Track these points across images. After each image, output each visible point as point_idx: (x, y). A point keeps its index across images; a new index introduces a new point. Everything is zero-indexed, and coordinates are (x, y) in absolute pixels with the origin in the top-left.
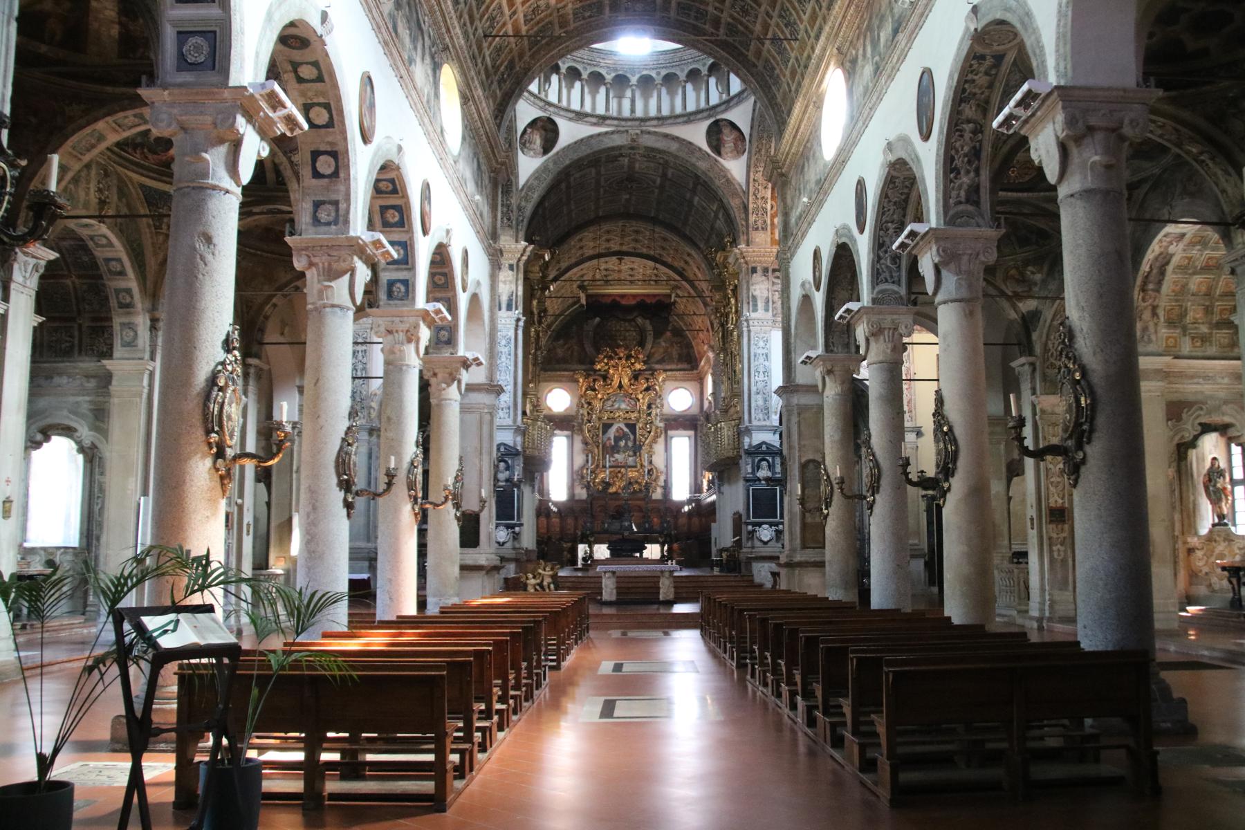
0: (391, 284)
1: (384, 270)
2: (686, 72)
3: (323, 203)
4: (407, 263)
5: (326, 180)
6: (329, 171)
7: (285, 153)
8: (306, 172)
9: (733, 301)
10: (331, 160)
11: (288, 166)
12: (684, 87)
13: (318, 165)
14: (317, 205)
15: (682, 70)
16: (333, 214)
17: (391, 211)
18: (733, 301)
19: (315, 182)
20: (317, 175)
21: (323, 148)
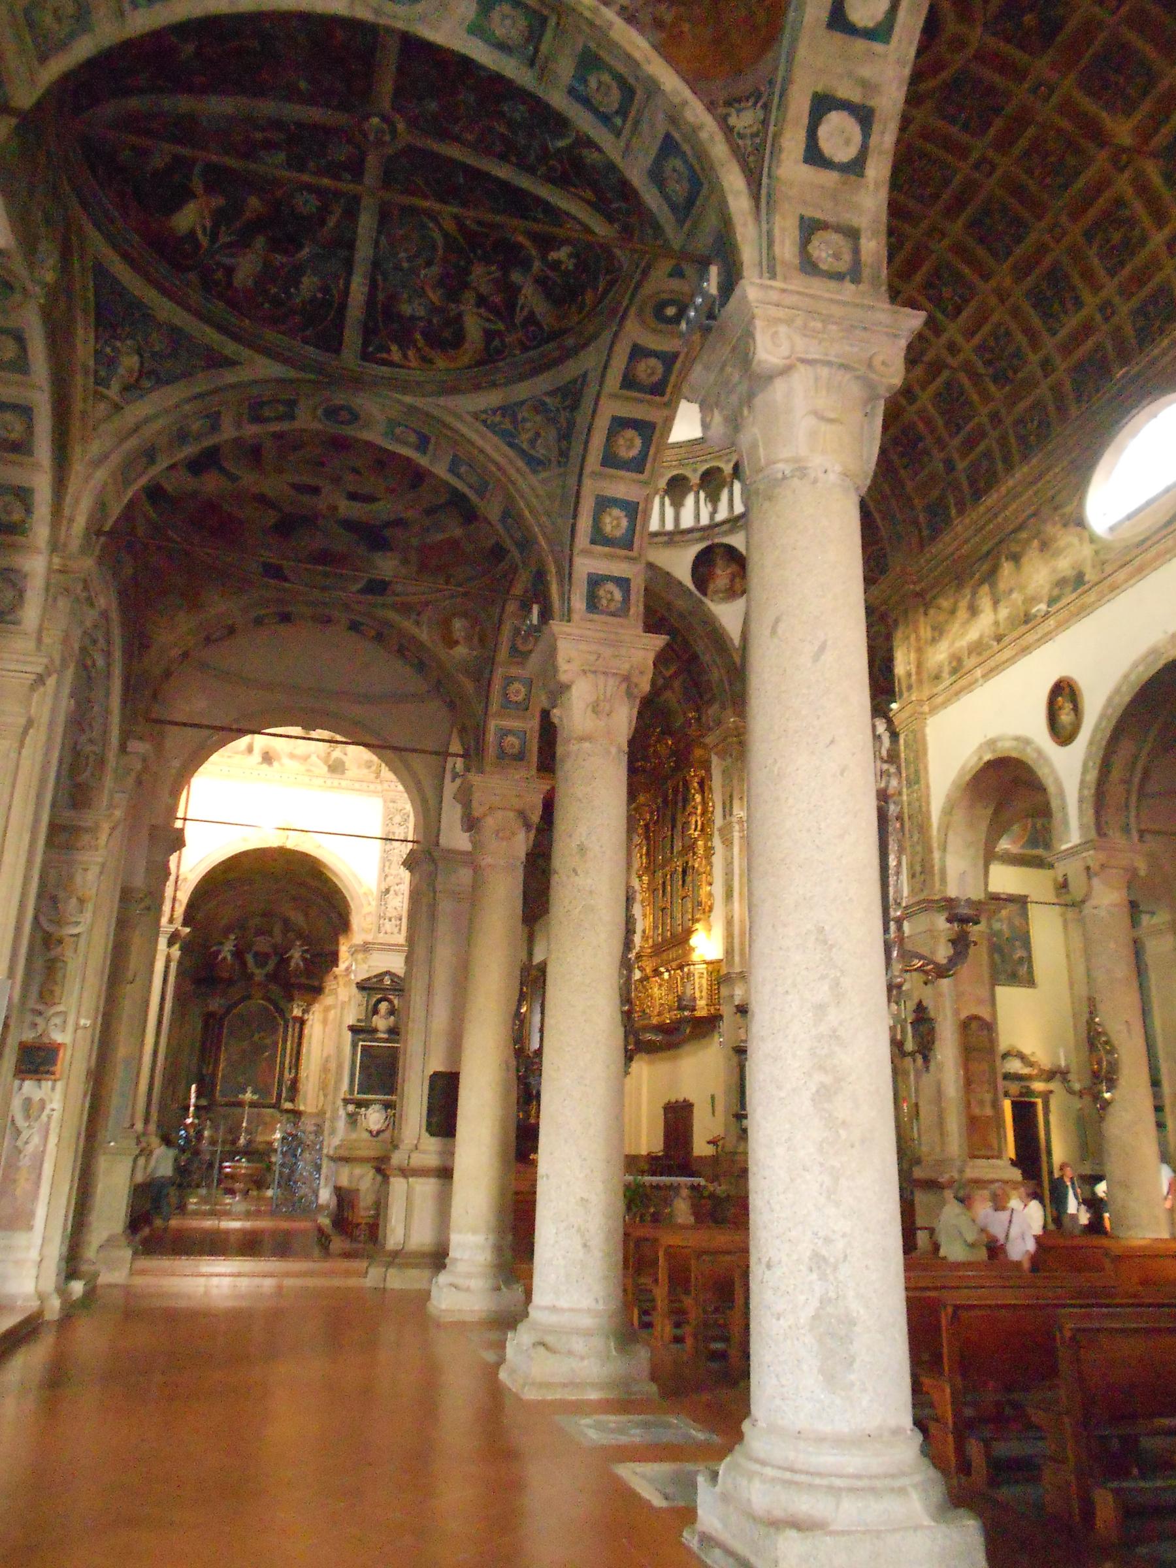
0: (595, 582)
1: (585, 552)
2: (700, 473)
3: (824, 226)
4: (630, 547)
5: (830, 178)
6: (844, 154)
7: (711, 107)
8: (793, 142)
9: (698, 798)
10: (854, 130)
11: (719, 137)
12: (697, 493)
13: (823, 131)
14: (809, 228)
15: (695, 470)
16: (847, 257)
17: (630, 433)
18: (698, 798)
19: (808, 173)
20: (814, 156)
21: (846, 91)
